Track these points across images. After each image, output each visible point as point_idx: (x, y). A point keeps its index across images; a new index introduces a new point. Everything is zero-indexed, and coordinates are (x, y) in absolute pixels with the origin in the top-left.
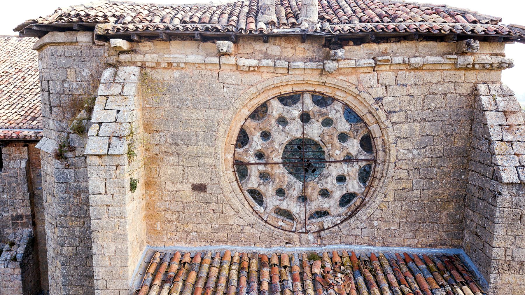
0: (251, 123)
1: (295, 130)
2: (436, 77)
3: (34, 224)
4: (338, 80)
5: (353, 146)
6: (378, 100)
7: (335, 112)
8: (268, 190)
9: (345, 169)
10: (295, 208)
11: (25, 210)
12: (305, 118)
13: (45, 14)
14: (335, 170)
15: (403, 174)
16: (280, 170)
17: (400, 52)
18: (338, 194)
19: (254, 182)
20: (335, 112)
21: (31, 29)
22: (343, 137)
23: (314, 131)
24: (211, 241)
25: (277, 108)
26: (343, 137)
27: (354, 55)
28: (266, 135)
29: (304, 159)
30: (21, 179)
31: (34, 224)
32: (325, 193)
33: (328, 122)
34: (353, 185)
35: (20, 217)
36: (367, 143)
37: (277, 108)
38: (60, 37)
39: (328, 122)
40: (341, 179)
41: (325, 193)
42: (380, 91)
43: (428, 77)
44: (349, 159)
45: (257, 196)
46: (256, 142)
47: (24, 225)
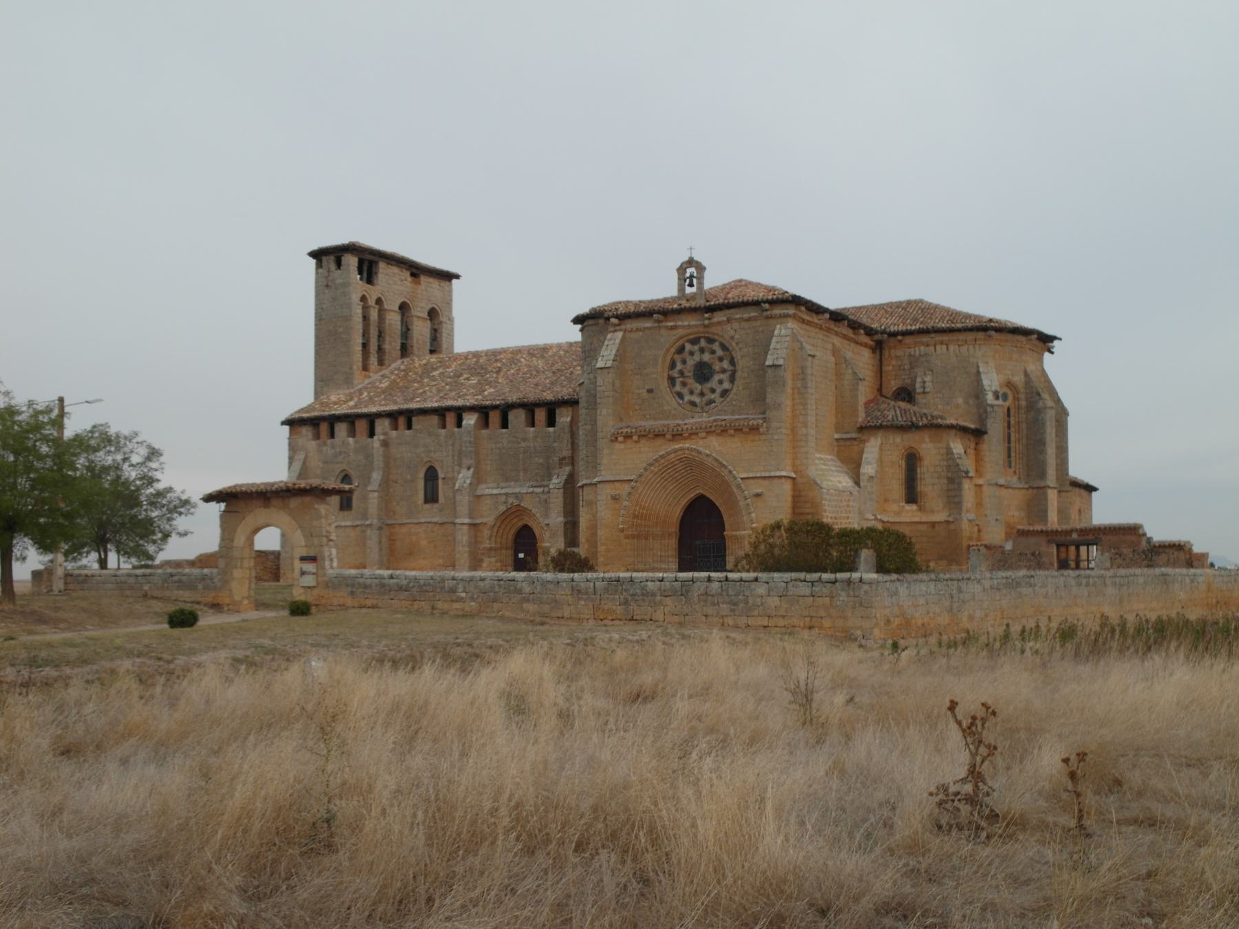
0: (676, 356)
1: (697, 358)
2: (759, 323)
3: (573, 464)
4: (713, 330)
5: (726, 364)
6: (732, 338)
7: (716, 346)
8: (685, 391)
9: (722, 376)
10: (697, 400)
11: (567, 453)
12: (702, 350)
13: (585, 310)
14: (716, 378)
15: (745, 375)
16: (691, 381)
17: (737, 314)
18: (719, 391)
19: (678, 388)
20: (716, 346)
21: (578, 320)
22: (721, 359)
23: (706, 357)
24: (655, 419)
25: (688, 347)
26: (721, 359)
27: (719, 317)
28: (684, 362)
29: (703, 373)
30: (567, 429)
31: (573, 464)
32: (713, 391)
33: (713, 352)
34: (726, 385)
35: (564, 458)
36: (732, 362)
37: (688, 347)
38: (591, 322)
39: (713, 352)
40: (721, 382)
41: (713, 391)
42: (732, 333)
43: (754, 324)
44: (724, 371)
45: (680, 395)
46: (679, 366)
47: (567, 465)
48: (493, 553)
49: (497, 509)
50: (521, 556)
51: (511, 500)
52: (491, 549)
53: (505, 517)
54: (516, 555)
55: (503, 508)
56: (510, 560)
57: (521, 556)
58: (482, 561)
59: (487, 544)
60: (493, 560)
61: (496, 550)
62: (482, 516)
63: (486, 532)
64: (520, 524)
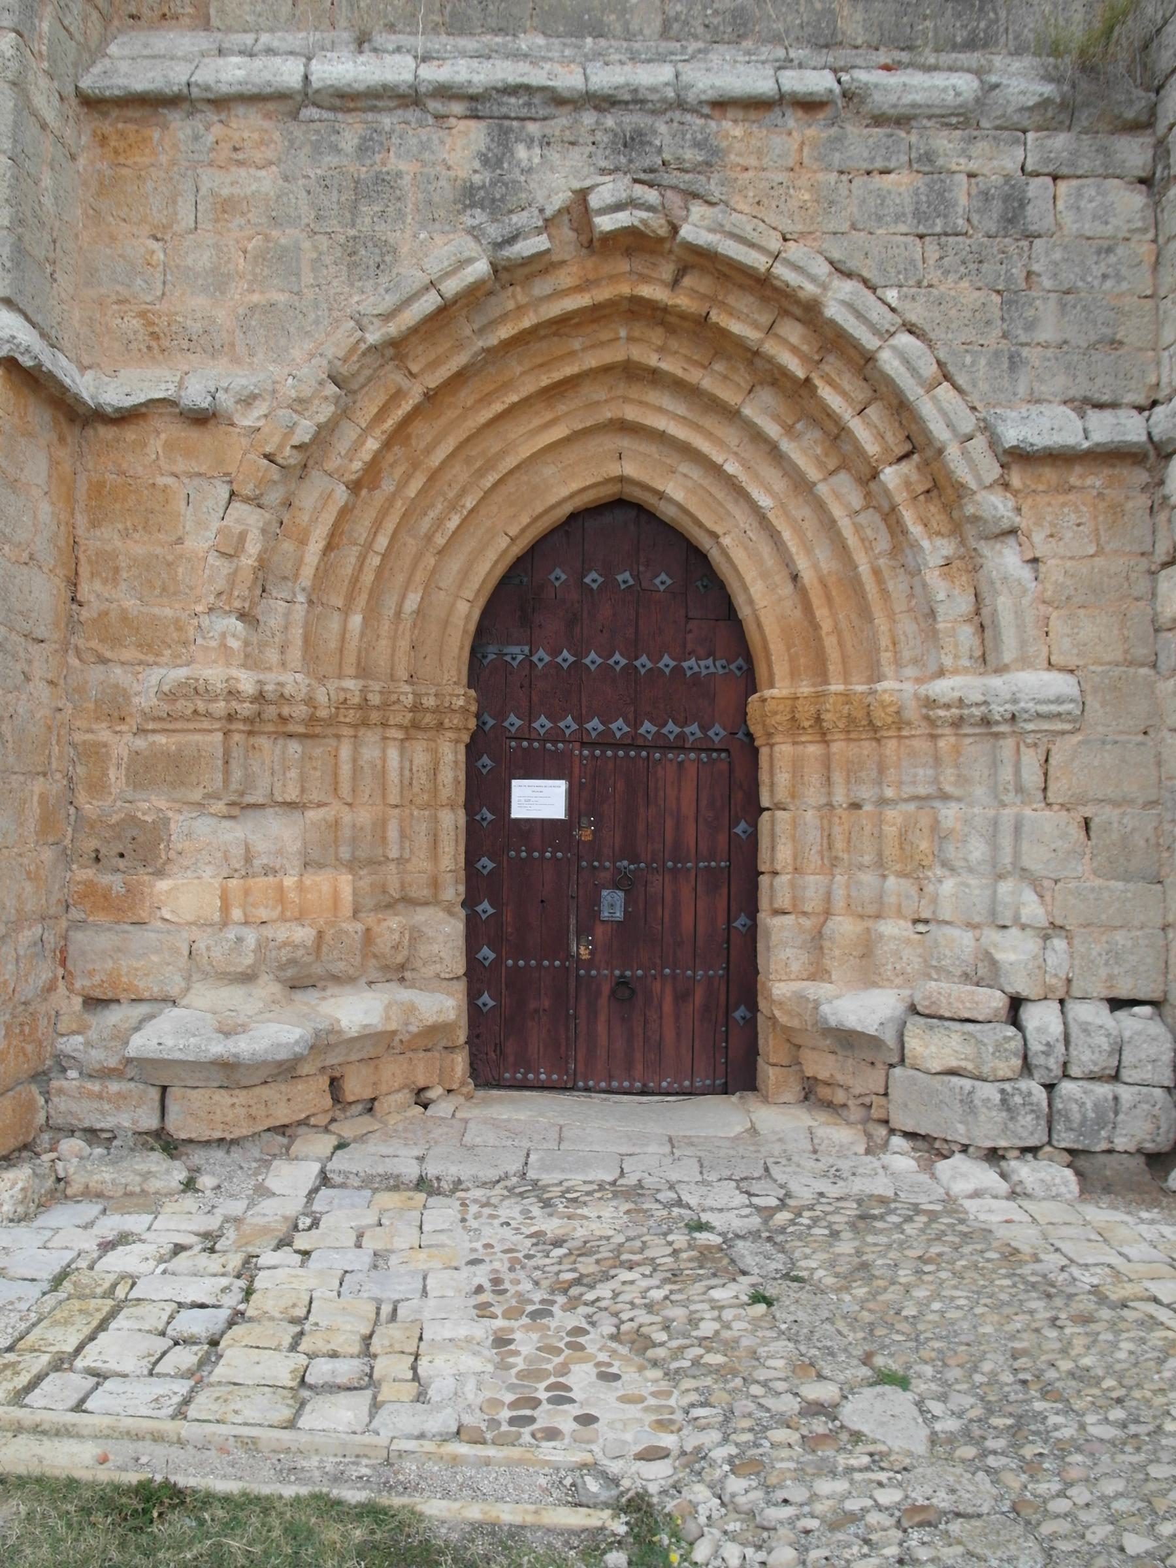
48: (276, 763)
49: (366, 257)
50: (539, 799)
51: (555, 174)
52: (261, 718)
53: (443, 364)
54: (484, 794)
55: (451, 257)
56: (438, 846)
57: (539, 799)
58: (143, 848)
59: (219, 660)
60: (277, 835)
61: (315, 729)
62: (158, 341)
63: (208, 525)
64: (566, 485)
